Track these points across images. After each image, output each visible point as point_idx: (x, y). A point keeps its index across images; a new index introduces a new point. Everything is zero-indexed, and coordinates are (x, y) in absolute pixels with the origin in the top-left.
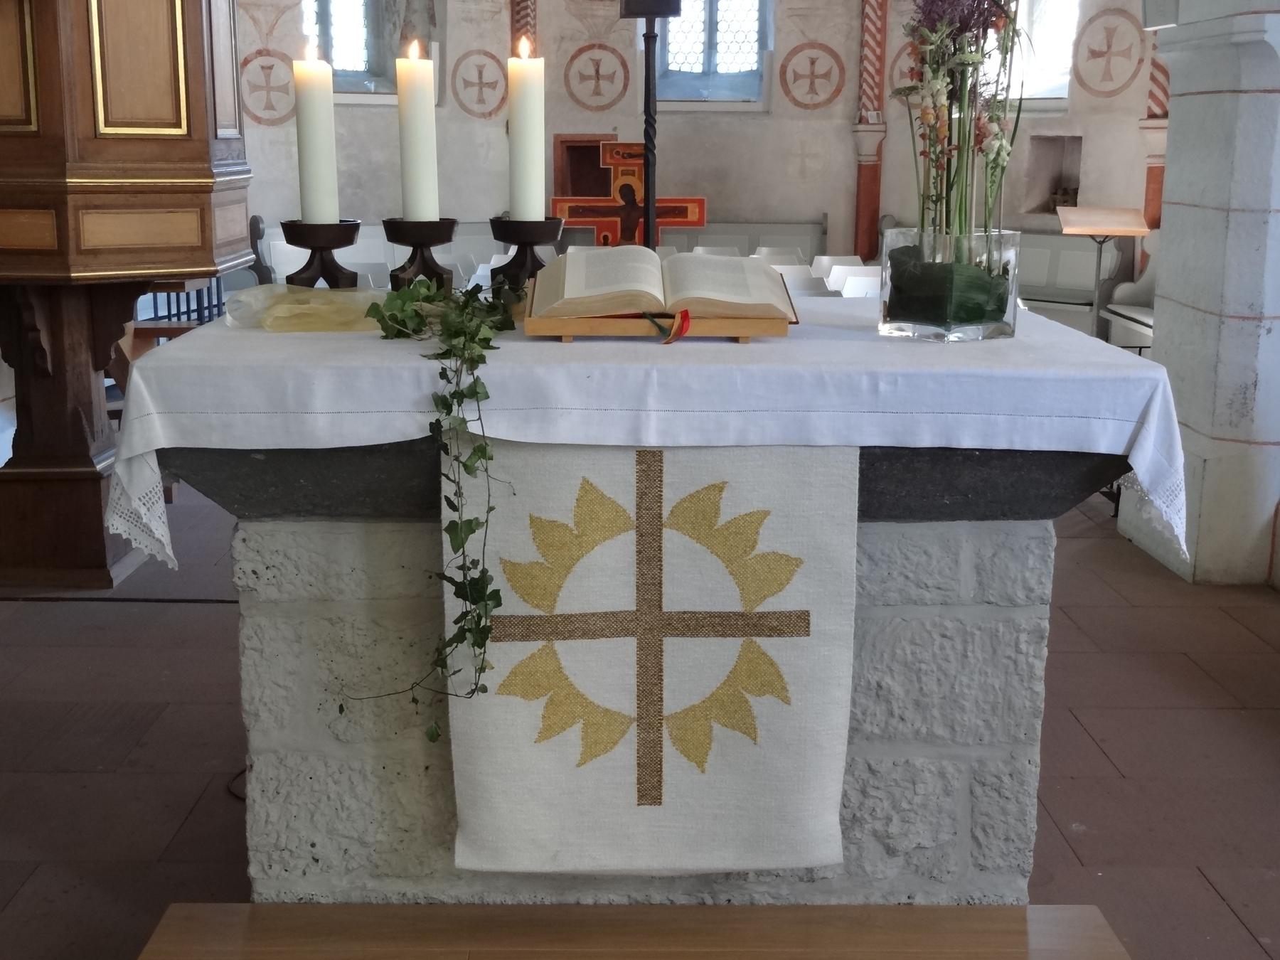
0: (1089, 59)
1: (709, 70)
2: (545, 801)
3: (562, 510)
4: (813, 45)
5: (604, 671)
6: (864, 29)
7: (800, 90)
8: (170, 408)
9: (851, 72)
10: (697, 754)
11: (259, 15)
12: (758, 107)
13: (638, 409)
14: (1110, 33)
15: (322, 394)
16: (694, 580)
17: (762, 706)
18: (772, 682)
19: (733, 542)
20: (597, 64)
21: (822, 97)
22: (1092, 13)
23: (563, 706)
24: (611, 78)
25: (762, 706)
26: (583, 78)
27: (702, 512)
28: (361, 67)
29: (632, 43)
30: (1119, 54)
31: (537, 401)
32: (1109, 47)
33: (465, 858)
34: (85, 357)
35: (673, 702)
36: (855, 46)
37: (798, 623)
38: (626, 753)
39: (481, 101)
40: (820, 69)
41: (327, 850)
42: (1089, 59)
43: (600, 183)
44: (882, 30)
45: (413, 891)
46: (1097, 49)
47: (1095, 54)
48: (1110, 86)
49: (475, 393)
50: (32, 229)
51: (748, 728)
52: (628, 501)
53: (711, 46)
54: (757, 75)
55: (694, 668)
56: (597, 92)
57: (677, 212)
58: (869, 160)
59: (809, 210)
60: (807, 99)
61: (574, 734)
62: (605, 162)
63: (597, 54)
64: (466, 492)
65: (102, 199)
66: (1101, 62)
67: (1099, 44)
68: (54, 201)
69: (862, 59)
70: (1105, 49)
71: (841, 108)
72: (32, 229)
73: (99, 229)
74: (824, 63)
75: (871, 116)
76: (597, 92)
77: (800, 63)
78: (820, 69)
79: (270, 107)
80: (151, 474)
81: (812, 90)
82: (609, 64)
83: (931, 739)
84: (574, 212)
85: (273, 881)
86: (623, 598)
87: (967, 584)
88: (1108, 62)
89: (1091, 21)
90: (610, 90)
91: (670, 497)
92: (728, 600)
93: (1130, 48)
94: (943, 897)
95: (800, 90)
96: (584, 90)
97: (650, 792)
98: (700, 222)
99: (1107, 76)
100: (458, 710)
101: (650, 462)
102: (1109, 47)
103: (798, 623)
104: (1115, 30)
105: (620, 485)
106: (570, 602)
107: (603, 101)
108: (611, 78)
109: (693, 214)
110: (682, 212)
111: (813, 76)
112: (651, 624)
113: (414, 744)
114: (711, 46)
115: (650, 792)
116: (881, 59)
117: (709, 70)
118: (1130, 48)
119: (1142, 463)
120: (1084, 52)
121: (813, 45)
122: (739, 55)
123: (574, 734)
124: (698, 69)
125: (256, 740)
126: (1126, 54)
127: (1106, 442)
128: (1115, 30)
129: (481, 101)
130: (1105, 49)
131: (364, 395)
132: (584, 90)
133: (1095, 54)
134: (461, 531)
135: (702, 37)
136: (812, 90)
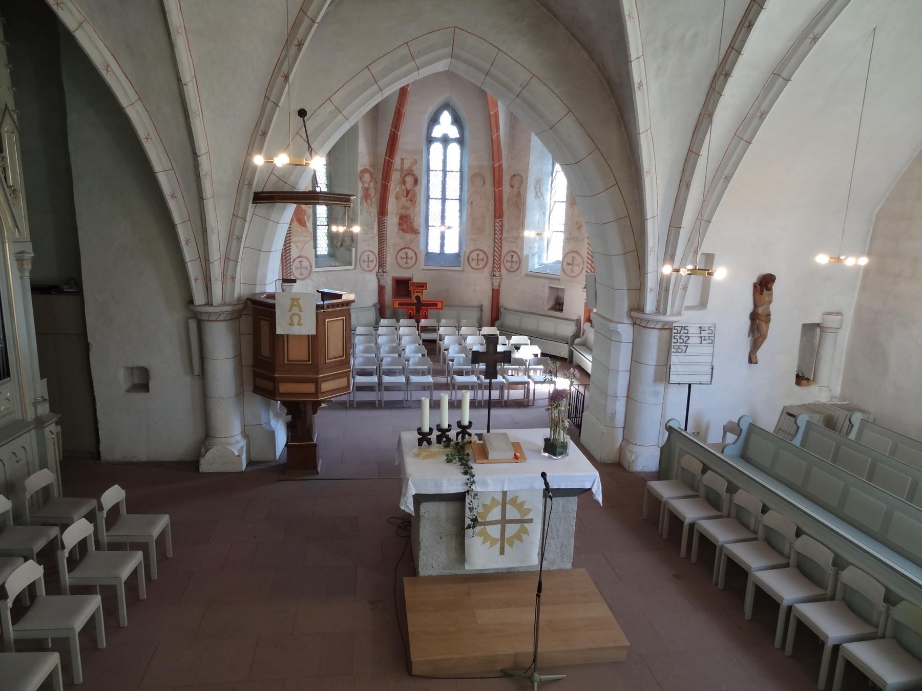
1: (442, 252)
2: (482, 556)
3: (488, 502)
4: (478, 250)
5: (494, 531)
6: (495, 246)
7: (474, 264)
8: (416, 486)
9: (491, 259)
10: (511, 545)
11: (299, 245)
12: (460, 268)
13: (503, 484)
14: (573, 258)
15: (445, 484)
16: (512, 513)
17: (524, 536)
18: (526, 532)
19: (519, 506)
20: (407, 254)
21: (481, 266)
23: (486, 537)
24: (411, 258)
25: (524, 536)
26: (402, 258)
27: (514, 502)
28: (326, 253)
29: (418, 247)
31: (485, 483)
33: (467, 567)
34: (311, 412)
35: (506, 536)
36: (492, 250)
37: (531, 521)
38: (498, 545)
39: (368, 267)
40: (480, 257)
41: (435, 565)
43: (408, 294)
44: (501, 247)
45: (452, 572)
47: (568, 264)
48: (572, 275)
49: (474, 482)
50: (310, 388)
51: (522, 541)
52: (500, 500)
53: (442, 245)
54: (458, 255)
55: (511, 529)
56: (407, 263)
57: (433, 305)
58: (495, 288)
59: (476, 303)
60: (476, 267)
61: (488, 543)
62: (411, 288)
63: (407, 250)
64: (468, 499)
65: (326, 379)
67: (570, 261)
68: (316, 382)
69: (494, 255)
71: (488, 270)
72: (310, 388)
73: (326, 386)
74: (482, 256)
75: (497, 274)
76: (407, 263)
77: (474, 255)
78: (480, 257)
79: (301, 274)
80: (411, 500)
81: (478, 264)
82: (411, 254)
83: (553, 538)
84: (400, 304)
85: (423, 571)
86: (499, 518)
87: (561, 508)
90: (411, 262)
91: (508, 499)
92: (518, 517)
94: (555, 568)
95: (474, 264)
96: (402, 262)
97: (502, 552)
98: (442, 308)
99: (572, 271)
100: (467, 540)
101: (504, 493)
103: (531, 521)
105: (499, 498)
106: (489, 519)
107: (408, 266)
108: (411, 258)
109: (439, 305)
110: (436, 305)
111: (478, 260)
112: (504, 521)
113: (453, 544)
114: (442, 245)
115: (502, 552)
116: (500, 255)
117: (442, 252)
119: (594, 490)
120: (565, 263)
121: (478, 250)
122: (452, 247)
123: (488, 543)
124: (438, 252)
125: (422, 544)
126: (578, 265)
127: (587, 486)
129: (368, 267)
131: (450, 481)
132: (402, 262)
133: (568, 264)
134: (471, 509)
135: (439, 241)
136: (478, 264)
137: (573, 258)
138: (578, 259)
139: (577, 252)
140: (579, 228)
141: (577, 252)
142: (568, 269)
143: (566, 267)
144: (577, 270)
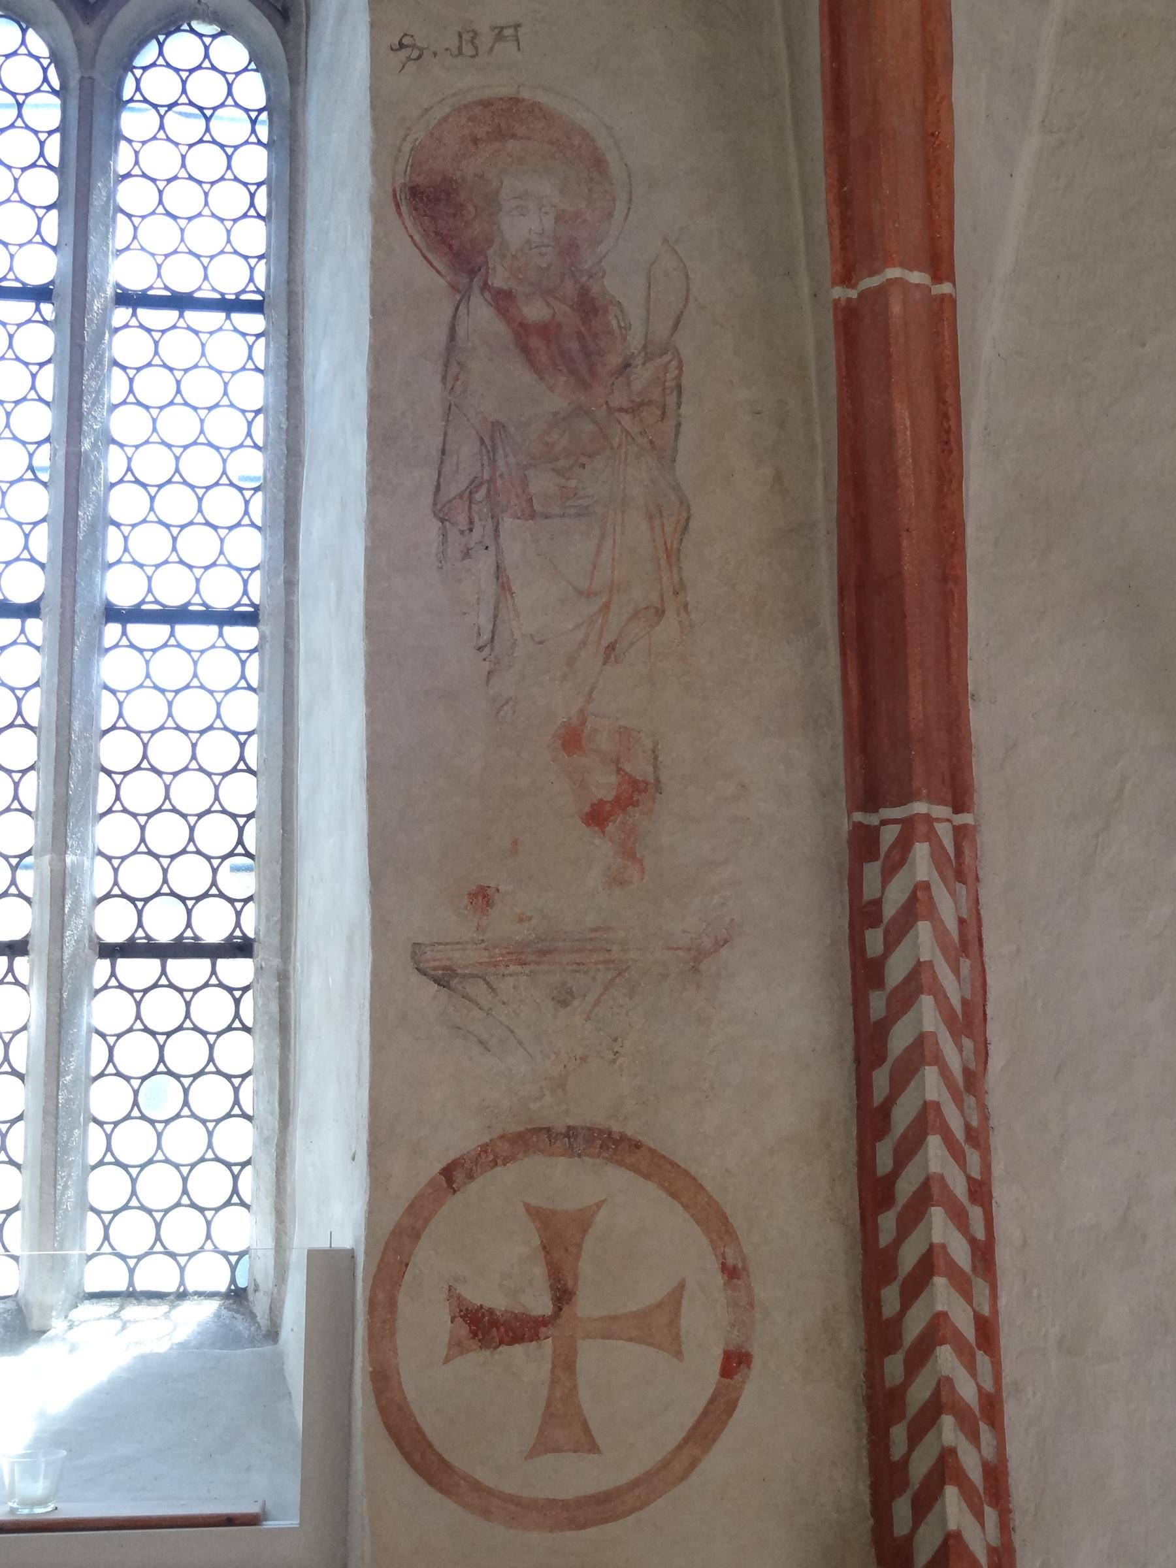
0: (457, 1348)
14: (559, 1240)
22: (462, 1138)
30: (610, 1328)
32: (563, 1295)
42: (457, 1348)
46: (496, 1301)
47: (484, 1328)
48: (575, 1476)
66: (529, 1363)
67: (508, 1276)
70: (540, 1304)
88: (565, 1364)
89: (451, 1175)
93: (676, 1297)
99: (564, 1424)
102: (563, 1295)
104: (584, 1220)
118: (676, 1297)
120: (426, 1321)
126: (658, 1326)
128: (584, 1220)
130: (540, 1304)
133: (484, 1328)
137: (559, 1240)
138: (642, 1242)
139: (611, 1145)
140: (618, 810)
141: (611, 1145)
142: (481, 1402)
143: (448, 1386)
144: (639, 1397)
